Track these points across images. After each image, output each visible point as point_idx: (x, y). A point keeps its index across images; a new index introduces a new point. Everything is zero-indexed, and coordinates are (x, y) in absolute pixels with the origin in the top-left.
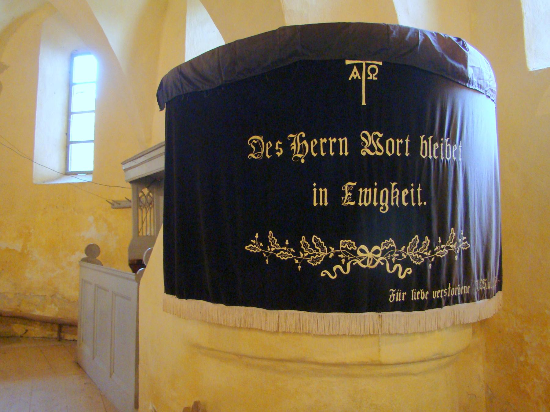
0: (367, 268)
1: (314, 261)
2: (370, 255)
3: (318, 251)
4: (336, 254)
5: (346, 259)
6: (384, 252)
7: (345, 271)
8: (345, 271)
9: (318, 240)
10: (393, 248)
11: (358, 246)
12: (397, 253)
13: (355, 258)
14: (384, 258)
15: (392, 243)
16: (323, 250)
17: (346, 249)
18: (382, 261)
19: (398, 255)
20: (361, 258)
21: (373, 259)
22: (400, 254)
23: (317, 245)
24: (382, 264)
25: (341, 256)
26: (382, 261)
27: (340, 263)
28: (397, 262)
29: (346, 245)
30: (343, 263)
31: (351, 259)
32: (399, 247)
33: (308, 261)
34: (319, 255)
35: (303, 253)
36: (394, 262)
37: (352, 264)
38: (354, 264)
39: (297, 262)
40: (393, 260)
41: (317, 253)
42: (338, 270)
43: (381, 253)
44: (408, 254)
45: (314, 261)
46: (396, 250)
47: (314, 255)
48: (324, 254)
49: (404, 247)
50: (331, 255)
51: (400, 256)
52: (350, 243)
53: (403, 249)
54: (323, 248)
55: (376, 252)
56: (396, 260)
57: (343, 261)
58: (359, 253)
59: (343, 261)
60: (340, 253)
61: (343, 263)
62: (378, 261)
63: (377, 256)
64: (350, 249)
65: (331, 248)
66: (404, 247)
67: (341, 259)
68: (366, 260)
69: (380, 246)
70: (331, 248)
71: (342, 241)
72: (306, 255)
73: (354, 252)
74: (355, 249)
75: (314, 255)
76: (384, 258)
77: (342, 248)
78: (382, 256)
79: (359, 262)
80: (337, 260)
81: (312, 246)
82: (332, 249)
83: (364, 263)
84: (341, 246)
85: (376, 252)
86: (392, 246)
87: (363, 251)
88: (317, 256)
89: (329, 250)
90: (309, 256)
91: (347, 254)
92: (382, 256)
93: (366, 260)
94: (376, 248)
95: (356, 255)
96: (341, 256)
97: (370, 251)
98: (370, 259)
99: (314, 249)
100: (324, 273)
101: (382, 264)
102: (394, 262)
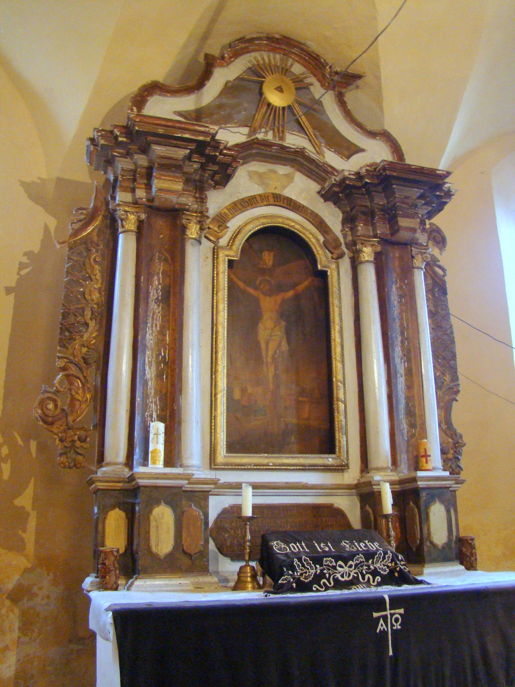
0: (346, 580)
1: (306, 578)
2: (346, 569)
3: (308, 569)
4: (322, 571)
5: (329, 574)
6: (356, 565)
7: (330, 584)
8: (330, 584)
9: (307, 560)
10: (363, 562)
11: (336, 562)
12: (366, 566)
13: (336, 573)
14: (356, 571)
15: (361, 557)
16: (311, 567)
17: (328, 565)
18: (355, 573)
19: (367, 567)
20: (340, 573)
21: (349, 573)
22: (369, 566)
23: (307, 564)
24: (356, 575)
25: (325, 571)
26: (355, 573)
27: (326, 578)
28: (367, 573)
29: (328, 562)
30: (327, 577)
31: (333, 574)
32: (367, 561)
33: (301, 579)
34: (309, 572)
35: (297, 572)
36: (365, 573)
37: (333, 577)
38: (336, 577)
39: (292, 580)
40: (364, 572)
41: (308, 571)
42: (324, 583)
43: (353, 567)
44: (375, 565)
45: (306, 578)
46: (365, 563)
47: (306, 573)
48: (313, 571)
49: (371, 560)
50: (319, 571)
51: (369, 568)
52: (330, 560)
53: (370, 562)
54: (312, 566)
55: (351, 566)
56: (366, 572)
57: (327, 575)
58: (338, 568)
59: (327, 575)
60: (324, 569)
61: (327, 577)
62: (352, 574)
63: (351, 569)
64: (331, 565)
65: (317, 565)
66: (371, 560)
67: (325, 574)
68: (343, 573)
69: (353, 561)
70: (317, 565)
71: (325, 559)
72: (299, 574)
73: (334, 568)
74: (335, 564)
75: (306, 573)
76: (356, 571)
77: (325, 565)
78: (355, 569)
79: (338, 576)
80: (322, 575)
81: (303, 565)
82: (318, 566)
83: (342, 576)
84: (324, 563)
85: (351, 566)
86: (362, 560)
87: (341, 566)
88: (308, 573)
89: (316, 568)
90: (301, 574)
91: (329, 570)
92: (355, 569)
93: (343, 573)
94: (351, 562)
95: (337, 570)
96: (325, 571)
97: (346, 566)
98: (346, 573)
99: (305, 567)
100: (315, 587)
101: (356, 575)
102: (365, 573)
